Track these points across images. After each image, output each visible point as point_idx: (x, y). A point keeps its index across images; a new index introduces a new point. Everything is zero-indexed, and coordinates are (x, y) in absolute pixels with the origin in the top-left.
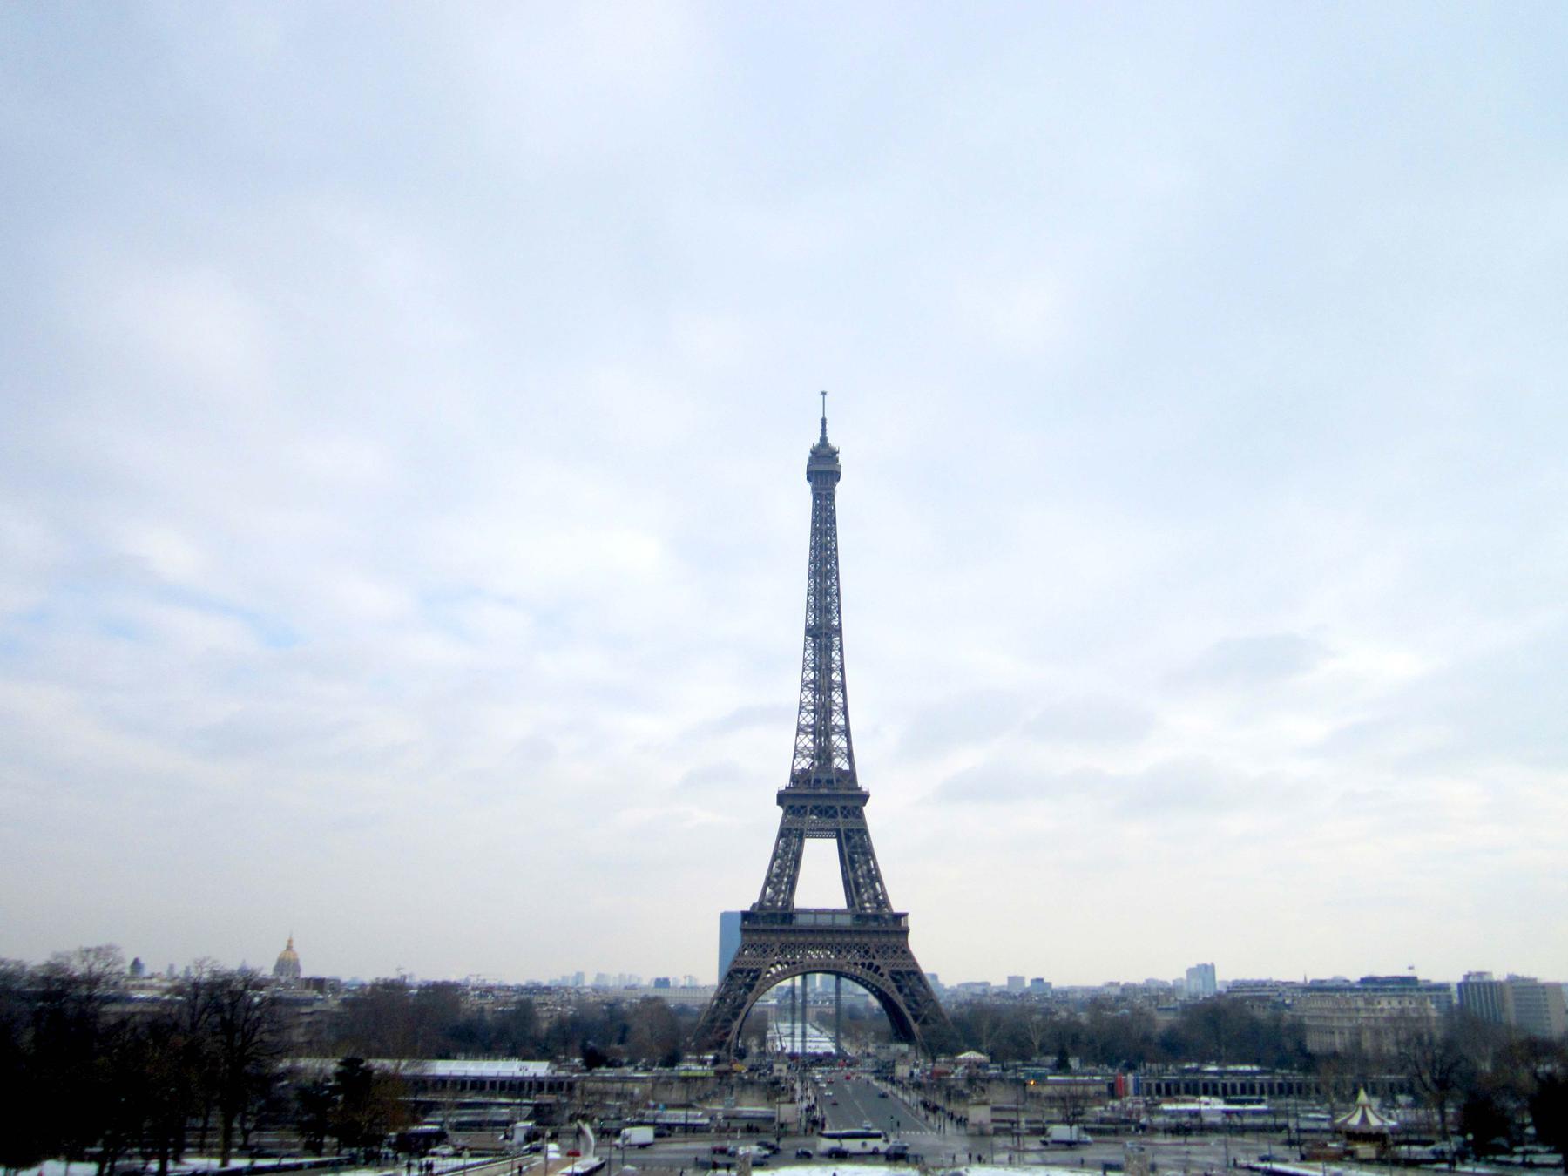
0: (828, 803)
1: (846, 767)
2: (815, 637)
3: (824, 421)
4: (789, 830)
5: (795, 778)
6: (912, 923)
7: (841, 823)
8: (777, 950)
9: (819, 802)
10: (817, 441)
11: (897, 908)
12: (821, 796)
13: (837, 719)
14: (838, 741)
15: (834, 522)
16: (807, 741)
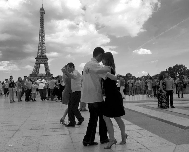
0: (42, 59)
1: (45, 55)
2: (41, 36)
3: (42, 4)
4: (37, 63)
5: (38, 56)
6: (53, 75)
7: (44, 62)
8: (34, 79)
9: (41, 59)
10: (41, 7)
11: (51, 73)
12: (41, 58)
13: (44, 48)
14: (44, 51)
15: (43, 20)
16: (40, 51)
